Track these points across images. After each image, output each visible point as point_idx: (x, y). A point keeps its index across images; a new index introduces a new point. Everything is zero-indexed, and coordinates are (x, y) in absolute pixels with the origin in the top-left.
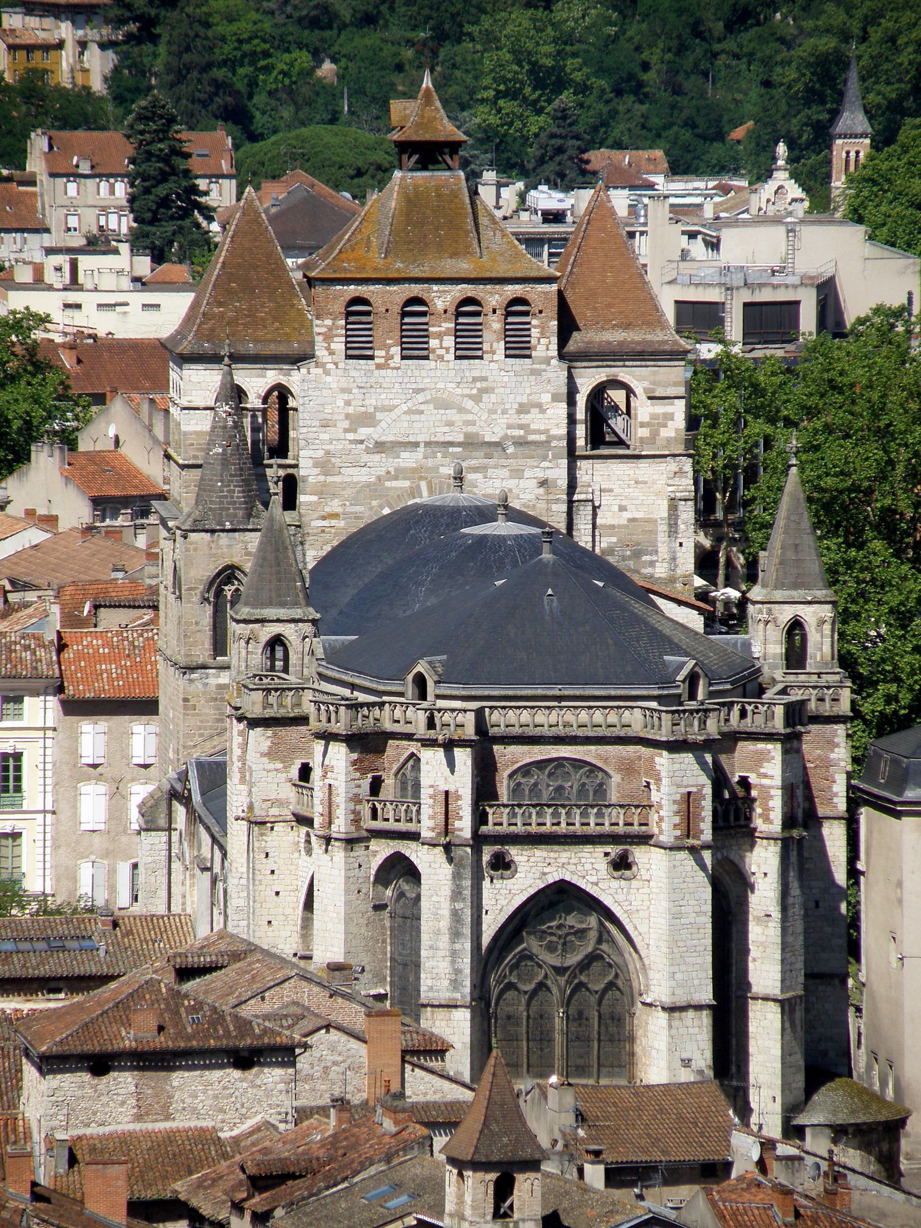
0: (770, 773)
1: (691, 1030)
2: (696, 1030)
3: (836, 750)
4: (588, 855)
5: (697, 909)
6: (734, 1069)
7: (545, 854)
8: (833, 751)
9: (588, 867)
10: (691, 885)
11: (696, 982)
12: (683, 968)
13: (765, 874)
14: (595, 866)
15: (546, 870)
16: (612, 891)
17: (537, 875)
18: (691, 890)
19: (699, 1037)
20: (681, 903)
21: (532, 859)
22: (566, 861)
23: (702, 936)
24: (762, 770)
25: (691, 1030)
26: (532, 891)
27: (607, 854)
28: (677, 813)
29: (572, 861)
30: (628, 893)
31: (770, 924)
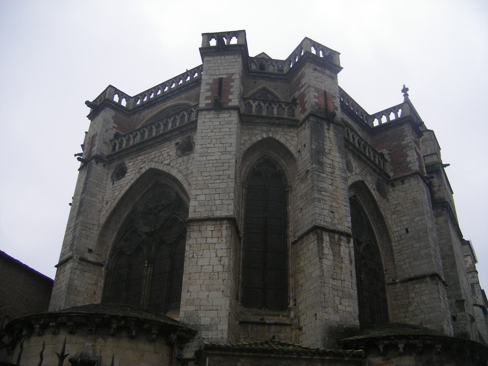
0: (304, 83)
1: (209, 240)
2: (215, 240)
3: (406, 139)
4: (166, 148)
5: (222, 150)
6: (292, 304)
7: (142, 157)
8: (404, 140)
9: (165, 155)
10: (217, 134)
11: (217, 202)
12: (206, 191)
13: (305, 145)
14: (170, 154)
15: (142, 166)
16: (177, 166)
17: (137, 171)
18: (219, 137)
19: (217, 246)
20: (208, 146)
21: (136, 162)
22: (153, 156)
23: (226, 168)
24: (300, 86)
25: (209, 240)
26: (132, 182)
27: (177, 144)
28: (208, 91)
29: (157, 155)
30: (187, 163)
31: (308, 177)
